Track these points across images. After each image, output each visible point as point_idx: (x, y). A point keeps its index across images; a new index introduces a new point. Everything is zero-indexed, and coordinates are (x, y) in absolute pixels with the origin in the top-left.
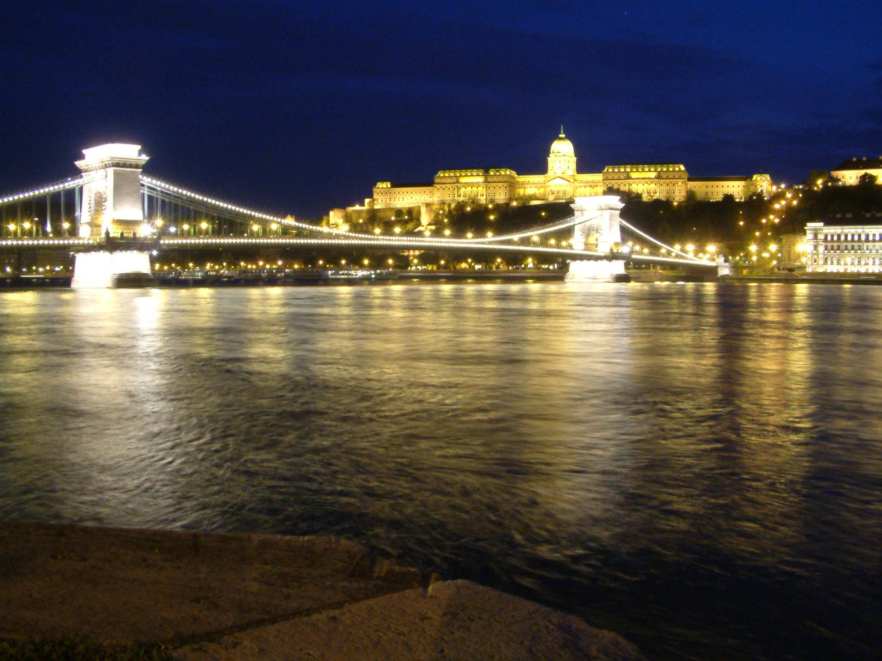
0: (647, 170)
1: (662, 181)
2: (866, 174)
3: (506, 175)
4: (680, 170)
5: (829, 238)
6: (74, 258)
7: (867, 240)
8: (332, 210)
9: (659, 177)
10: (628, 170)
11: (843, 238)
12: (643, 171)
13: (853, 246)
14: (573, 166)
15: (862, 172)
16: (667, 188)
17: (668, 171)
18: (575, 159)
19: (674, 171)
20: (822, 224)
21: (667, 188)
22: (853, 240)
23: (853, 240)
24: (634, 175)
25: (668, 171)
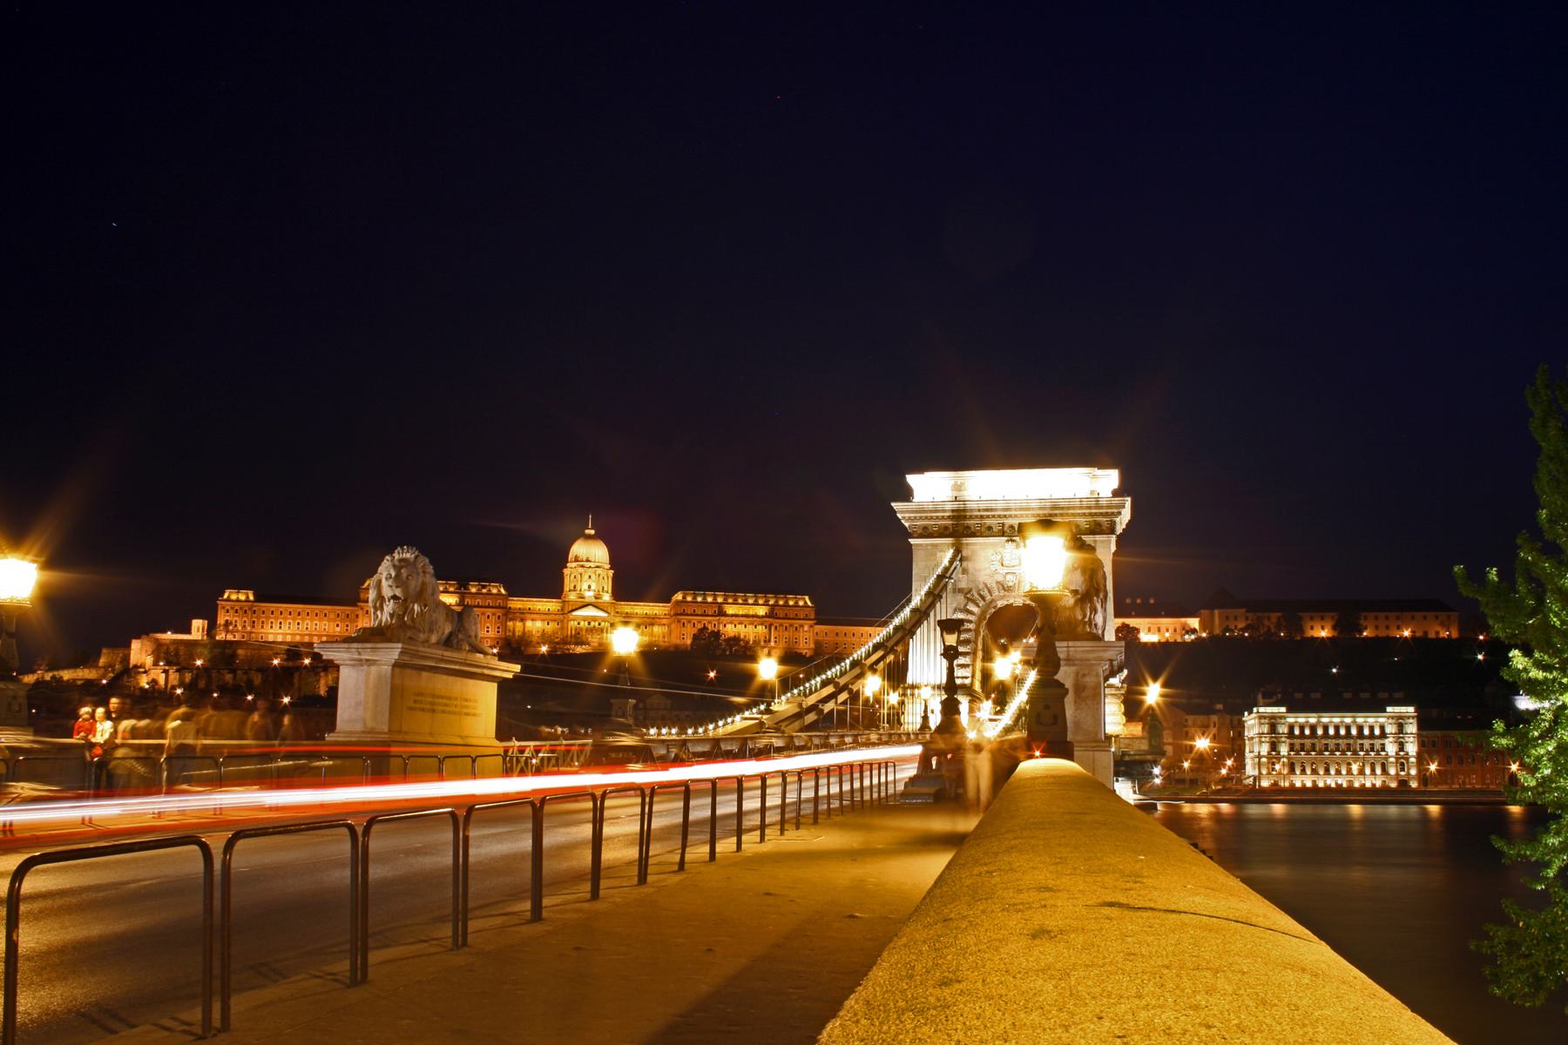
3: (499, 594)
4: (806, 605)
5: (1297, 732)
7: (1360, 734)
8: (138, 637)
9: (769, 615)
10: (720, 600)
11: (1320, 732)
12: (745, 603)
13: (1313, 745)
14: (608, 586)
17: (786, 605)
18: (611, 573)
20: (1283, 709)
22: (1372, 736)
24: (730, 610)
25: (786, 605)
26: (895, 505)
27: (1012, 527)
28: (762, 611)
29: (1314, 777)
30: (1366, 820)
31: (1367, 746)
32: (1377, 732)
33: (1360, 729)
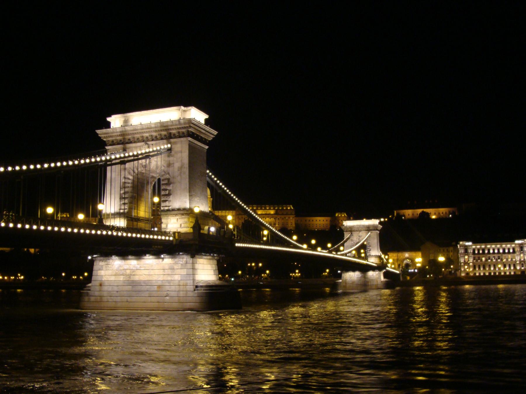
0: (268, 208)
1: (279, 217)
2: (423, 212)
5: (476, 252)
6: (92, 262)
7: (504, 252)
9: (276, 213)
10: (255, 208)
11: (486, 252)
12: (265, 209)
15: (419, 211)
16: (283, 221)
17: (283, 209)
19: (287, 209)
21: (283, 221)
23: (494, 253)
25: (283, 209)
26: (98, 131)
27: (147, 137)
28: (272, 212)
29: (484, 271)
30: (505, 290)
31: (496, 257)
32: (511, 251)
33: (504, 250)
